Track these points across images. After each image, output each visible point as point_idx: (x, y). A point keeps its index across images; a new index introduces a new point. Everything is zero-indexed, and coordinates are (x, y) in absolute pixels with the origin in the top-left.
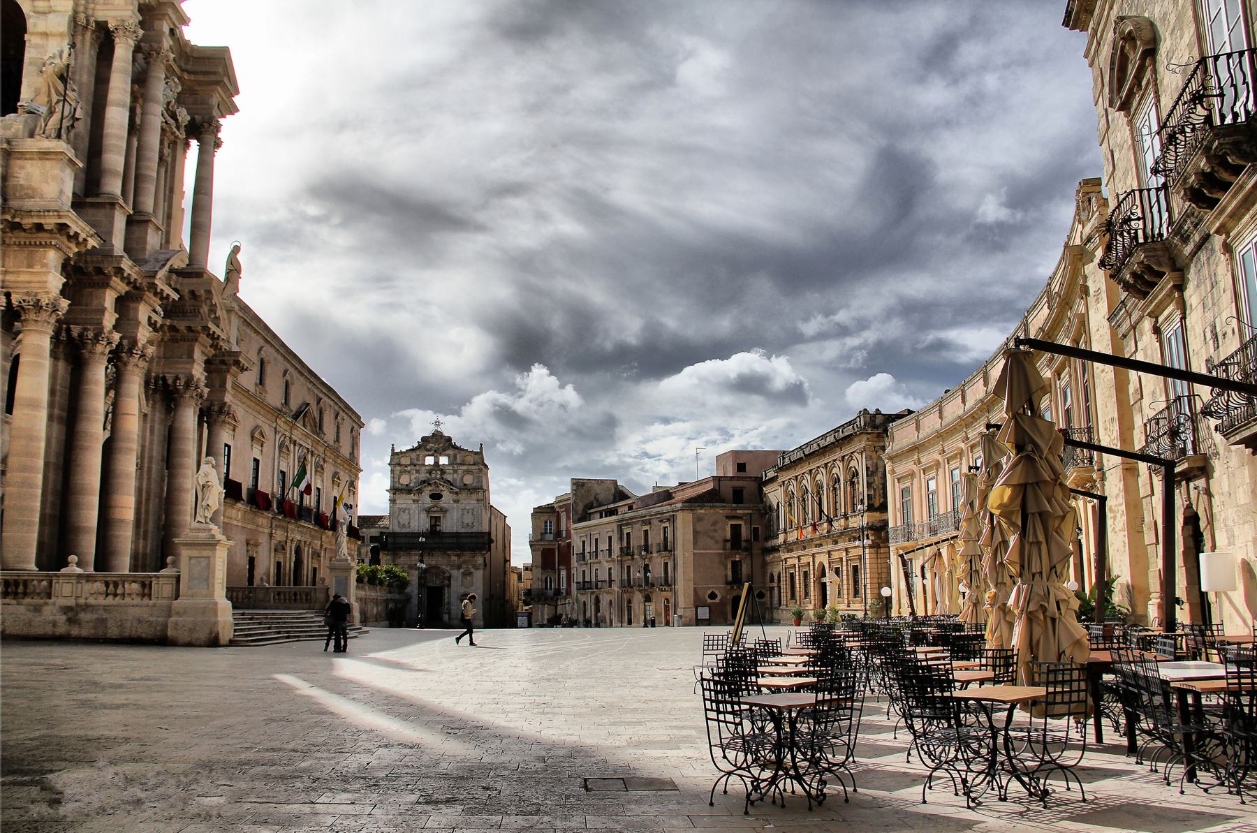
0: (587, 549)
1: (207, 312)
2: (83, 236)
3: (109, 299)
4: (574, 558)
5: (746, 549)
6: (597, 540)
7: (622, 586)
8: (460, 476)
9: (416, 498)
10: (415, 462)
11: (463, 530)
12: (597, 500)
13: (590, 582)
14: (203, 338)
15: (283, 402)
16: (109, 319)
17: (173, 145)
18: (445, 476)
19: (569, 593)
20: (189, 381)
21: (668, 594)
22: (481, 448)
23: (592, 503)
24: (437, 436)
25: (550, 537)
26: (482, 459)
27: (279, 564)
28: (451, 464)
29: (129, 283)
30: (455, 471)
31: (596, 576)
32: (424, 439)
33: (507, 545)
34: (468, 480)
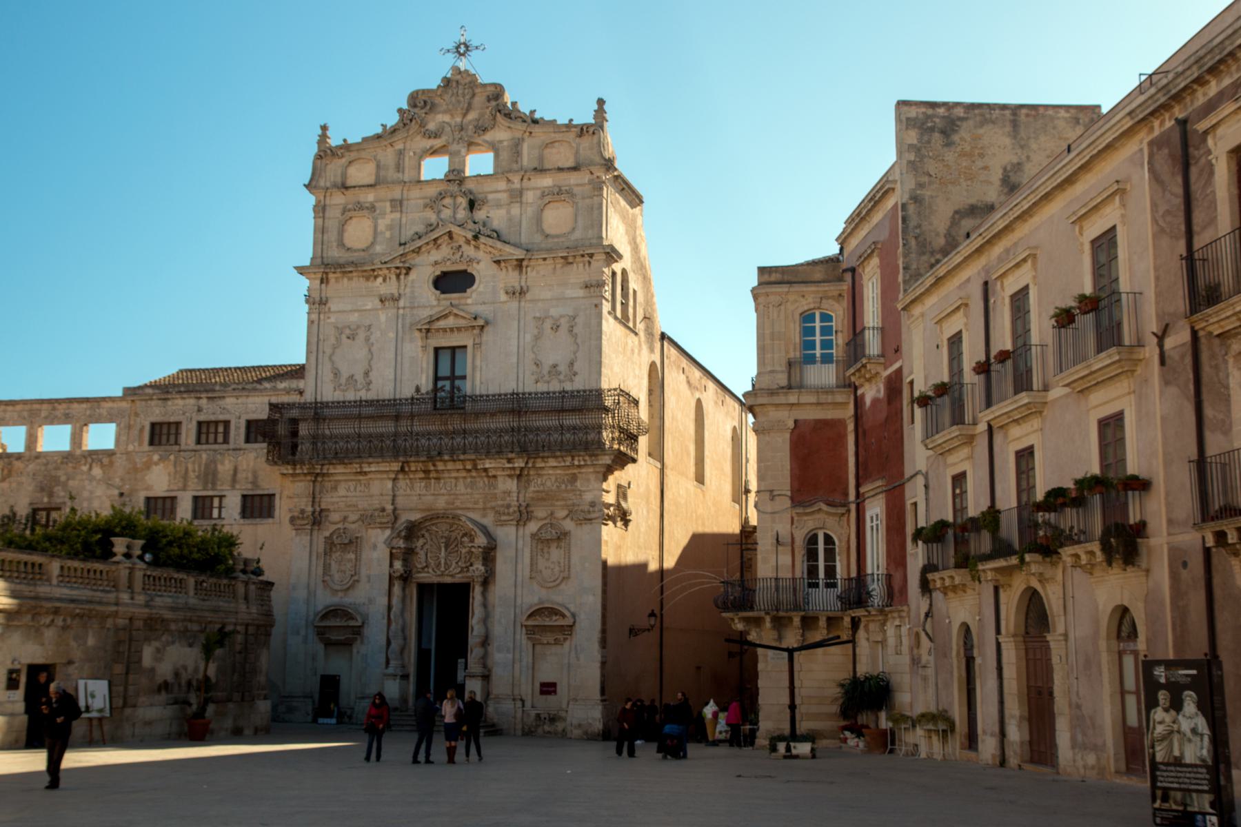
8: (530, 211)
9: (390, 288)
10: (391, 174)
11: (542, 387)
25: (823, 375)
26: (600, 145)
28: (501, 171)
30: (517, 196)
32: (421, 103)
34: (558, 218)
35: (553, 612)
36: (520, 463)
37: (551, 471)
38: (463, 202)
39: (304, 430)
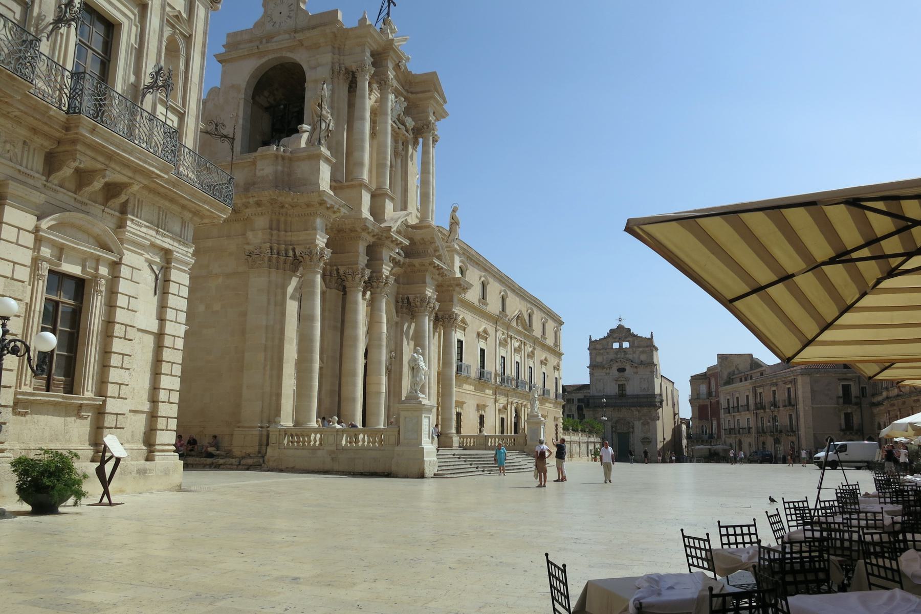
0: (731, 405)
1: (433, 251)
2: (337, 206)
3: (362, 248)
4: (722, 412)
5: (856, 404)
6: (738, 398)
7: (758, 432)
9: (608, 371)
11: (641, 393)
12: (738, 369)
13: (734, 429)
14: (431, 268)
15: (501, 310)
16: (363, 260)
17: (405, 144)
18: (627, 356)
19: (719, 437)
20: (424, 300)
21: (794, 438)
22: (652, 335)
23: (734, 372)
24: (620, 328)
27: (502, 420)
29: (374, 236)
30: (634, 352)
31: (739, 425)
32: (612, 331)
33: (676, 403)
34: (643, 357)
35: (647, 438)
36: (639, 408)
37: (645, 410)
38: (623, 353)
39: (591, 401)
